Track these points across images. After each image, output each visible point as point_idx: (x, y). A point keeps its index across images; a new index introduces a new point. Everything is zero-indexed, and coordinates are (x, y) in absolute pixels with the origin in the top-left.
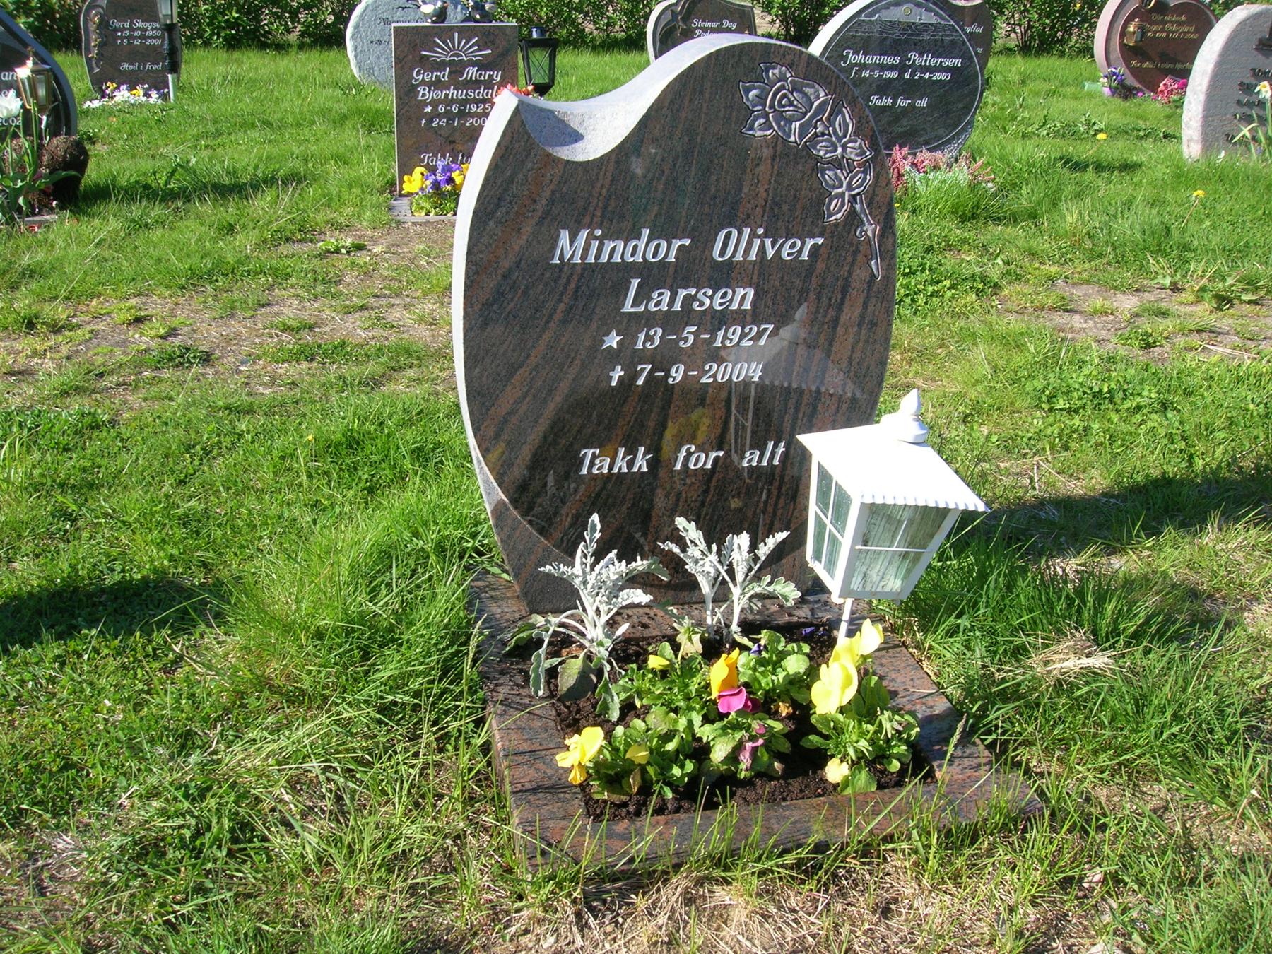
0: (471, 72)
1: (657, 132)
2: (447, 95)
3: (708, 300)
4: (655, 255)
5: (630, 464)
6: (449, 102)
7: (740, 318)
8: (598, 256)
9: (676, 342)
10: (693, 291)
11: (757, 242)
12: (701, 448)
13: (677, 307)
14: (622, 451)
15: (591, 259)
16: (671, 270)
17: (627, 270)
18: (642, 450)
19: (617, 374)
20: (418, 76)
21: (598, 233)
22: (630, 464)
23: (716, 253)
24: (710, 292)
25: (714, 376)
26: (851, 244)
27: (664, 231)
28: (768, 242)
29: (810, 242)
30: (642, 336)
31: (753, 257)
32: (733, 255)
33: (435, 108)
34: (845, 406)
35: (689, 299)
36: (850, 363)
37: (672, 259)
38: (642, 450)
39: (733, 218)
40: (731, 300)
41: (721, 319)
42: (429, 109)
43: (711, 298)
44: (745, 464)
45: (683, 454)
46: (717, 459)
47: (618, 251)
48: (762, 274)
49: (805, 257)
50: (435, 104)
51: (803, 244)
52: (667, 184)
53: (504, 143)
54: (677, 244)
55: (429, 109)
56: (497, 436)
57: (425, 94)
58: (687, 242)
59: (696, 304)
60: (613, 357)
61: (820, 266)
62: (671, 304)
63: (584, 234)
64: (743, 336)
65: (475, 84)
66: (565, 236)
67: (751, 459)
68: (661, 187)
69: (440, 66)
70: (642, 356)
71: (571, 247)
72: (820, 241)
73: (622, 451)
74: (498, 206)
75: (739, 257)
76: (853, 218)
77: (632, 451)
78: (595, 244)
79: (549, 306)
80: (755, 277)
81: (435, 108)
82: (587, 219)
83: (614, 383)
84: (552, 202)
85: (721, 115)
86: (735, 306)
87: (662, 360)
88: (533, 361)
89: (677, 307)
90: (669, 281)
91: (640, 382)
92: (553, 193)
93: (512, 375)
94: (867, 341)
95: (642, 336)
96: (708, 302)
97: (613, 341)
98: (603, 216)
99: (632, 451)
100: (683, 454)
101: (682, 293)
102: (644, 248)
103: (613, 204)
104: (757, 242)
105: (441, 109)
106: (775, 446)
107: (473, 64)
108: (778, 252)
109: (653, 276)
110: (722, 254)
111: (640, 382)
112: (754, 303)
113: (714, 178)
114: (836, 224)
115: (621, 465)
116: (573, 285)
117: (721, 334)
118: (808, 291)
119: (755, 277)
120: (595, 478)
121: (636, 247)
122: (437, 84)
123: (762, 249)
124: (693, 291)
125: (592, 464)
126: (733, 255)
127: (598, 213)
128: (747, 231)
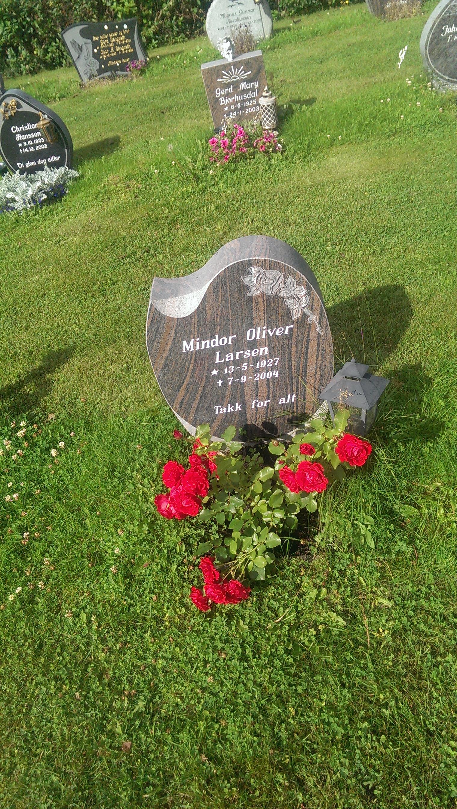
0: (243, 86)
1: (211, 302)
2: (234, 100)
3: (247, 354)
4: (223, 343)
5: (234, 408)
6: (236, 103)
7: (264, 357)
8: (200, 346)
9: (240, 369)
10: (242, 352)
11: (264, 332)
12: (261, 400)
13: (237, 358)
14: (229, 405)
15: (198, 348)
16: (231, 346)
17: (213, 350)
18: (237, 404)
19: (220, 382)
20: (219, 92)
21: (198, 339)
22: (234, 408)
23: (248, 339)
24: (249, 351)
25: (259, 377)
26: (307, 325)
27: (224, 333)
28: (269, 331)
29: (287, 328)
30: (226, 370)
31: (264, 337)
32: (256, 337)
33: (229, 108)
34: (318, 379)
35: (241, 356)
36: (317, 365)
37: (230, 343)
38: (237, 404)
39: (251, 325)
40: (259, 352)
41: (257, 359)
42: (226, 109)
43: (250, 353)
44: (280, 403)
45: (254, 403)
46: (268, 403)
47: (207, 344)
48: (270, 341)
49: (286, 333)
50: (229, 105)
51: (285, 329)
52: (220, 318)
53: (151, 317)
54: (230, 338)
55: (226, 109)
56: (181, 407)
57: (223, 101)
58: (235, 336)
59: (245, 356)
60: (217, 377)
61: (295, 335)
62: (235, 357)
63: (192, 341)
64: (267, 363)
65: (246, 91)
66: (185, 343)
67: (282, 401)
68: (218, 320)
69: (228, 85)
70: (228, 375)
71: (189, 346)
72: (292, 326)
73: (229, 405)
74: (156, 338)
75: (258, 338)
76: (304, 316)
77: (233, 404)
78: (198, 344)
79: (187, 365)
80: (267, 344)
81: (229, 108)
82: (192, 336)
83: (220, 385)
84: (176, 333)
85: (236, 290)
86: (261, 354)
87: (238, 374)
88: (186, 383)
89: (237, 358)
90: (232, 350)
91: (230, 383)
92: (176, 330)
93: (180, 388)
94: (322, 357)
95: (226, 370)
96: (249, 355)
97: (215, 372)
98: (198, 334)
99: (233, 404)
100: (254, 403)
101: (238, 353)
102: (217, 341)
103: (200, 329)
104: (264, 332)
105: (232, 107)
106: (291, 396)
107: (243, 81)
108: (275, 334)
109: (224, 350)
110: (251, 337)
111: (230, 383)
112: (269, 352)
113: (240, 313)
114: (298, 319)
115: (230, 409)
116: (194, 358)
117: (258, 364)
118: (291, 344)
119: (267, 344)
120: (222, 414)
121: (214, 342)
122: (228, 95)
123: (267, 334)
124: (242, 352)
125: (219, 411)
126: (256, 337)
127: (196, 333)
128: (259, 329)
